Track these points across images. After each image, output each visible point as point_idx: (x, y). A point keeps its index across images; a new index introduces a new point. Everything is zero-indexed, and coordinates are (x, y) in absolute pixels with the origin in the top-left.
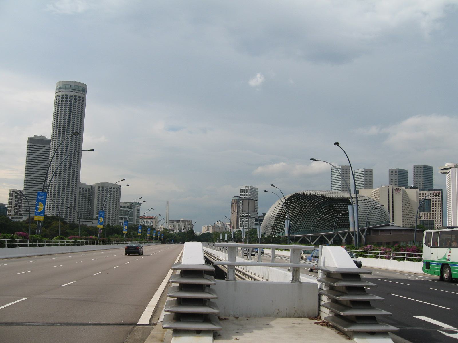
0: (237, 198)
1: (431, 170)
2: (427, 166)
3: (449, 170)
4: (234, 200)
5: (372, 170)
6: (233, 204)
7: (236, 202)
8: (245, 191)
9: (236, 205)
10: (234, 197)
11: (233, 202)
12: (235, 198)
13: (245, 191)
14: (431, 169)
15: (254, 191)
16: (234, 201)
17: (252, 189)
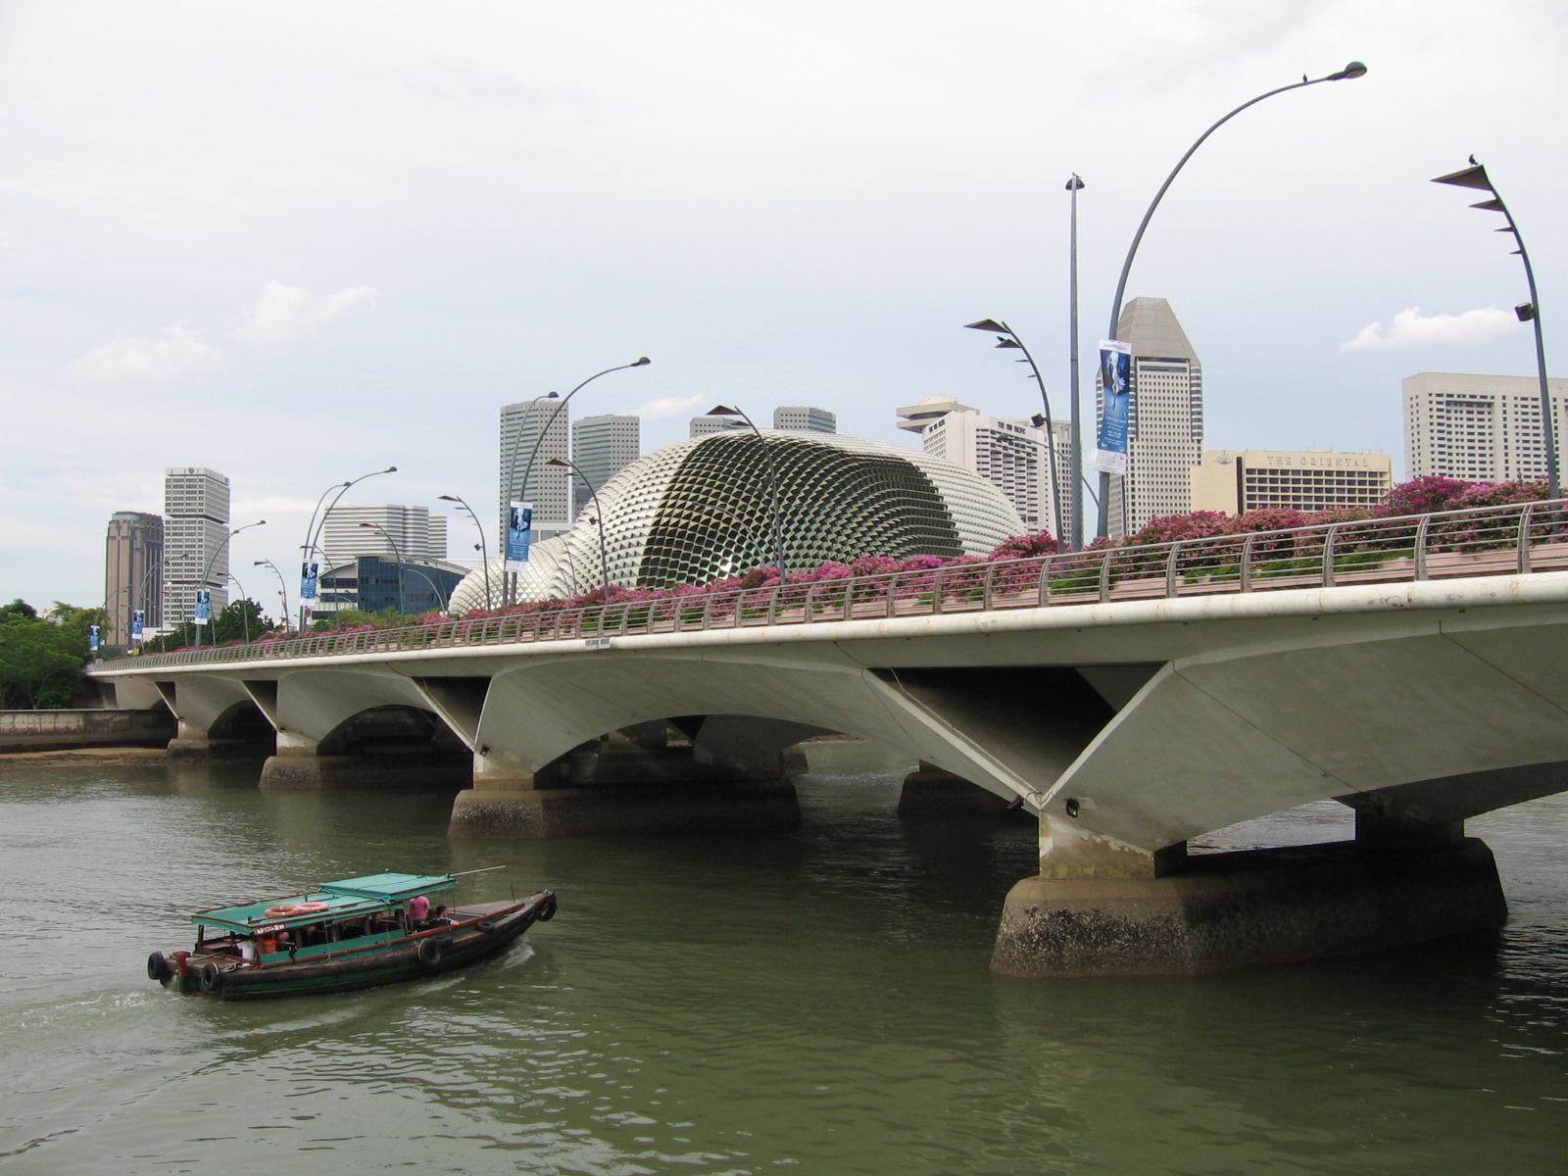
0: (129, 517)
1: (830, 424)
2: (820, 411)
3: (940, 419)
4: (118, 522)
5: (638, 419)
6: (114, 538)
7: (125, 532)
8: (182, 487)
9: (127, 542)
10: (118, 513)
11: (114, 533)
12: (120, 518)
13: (182, 487)
14: (831, 421)
15: (216, 487)
16: (119, 528)
17: (210, 477)
